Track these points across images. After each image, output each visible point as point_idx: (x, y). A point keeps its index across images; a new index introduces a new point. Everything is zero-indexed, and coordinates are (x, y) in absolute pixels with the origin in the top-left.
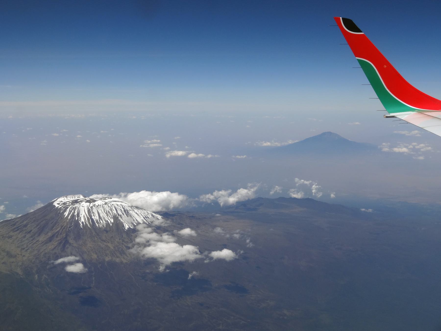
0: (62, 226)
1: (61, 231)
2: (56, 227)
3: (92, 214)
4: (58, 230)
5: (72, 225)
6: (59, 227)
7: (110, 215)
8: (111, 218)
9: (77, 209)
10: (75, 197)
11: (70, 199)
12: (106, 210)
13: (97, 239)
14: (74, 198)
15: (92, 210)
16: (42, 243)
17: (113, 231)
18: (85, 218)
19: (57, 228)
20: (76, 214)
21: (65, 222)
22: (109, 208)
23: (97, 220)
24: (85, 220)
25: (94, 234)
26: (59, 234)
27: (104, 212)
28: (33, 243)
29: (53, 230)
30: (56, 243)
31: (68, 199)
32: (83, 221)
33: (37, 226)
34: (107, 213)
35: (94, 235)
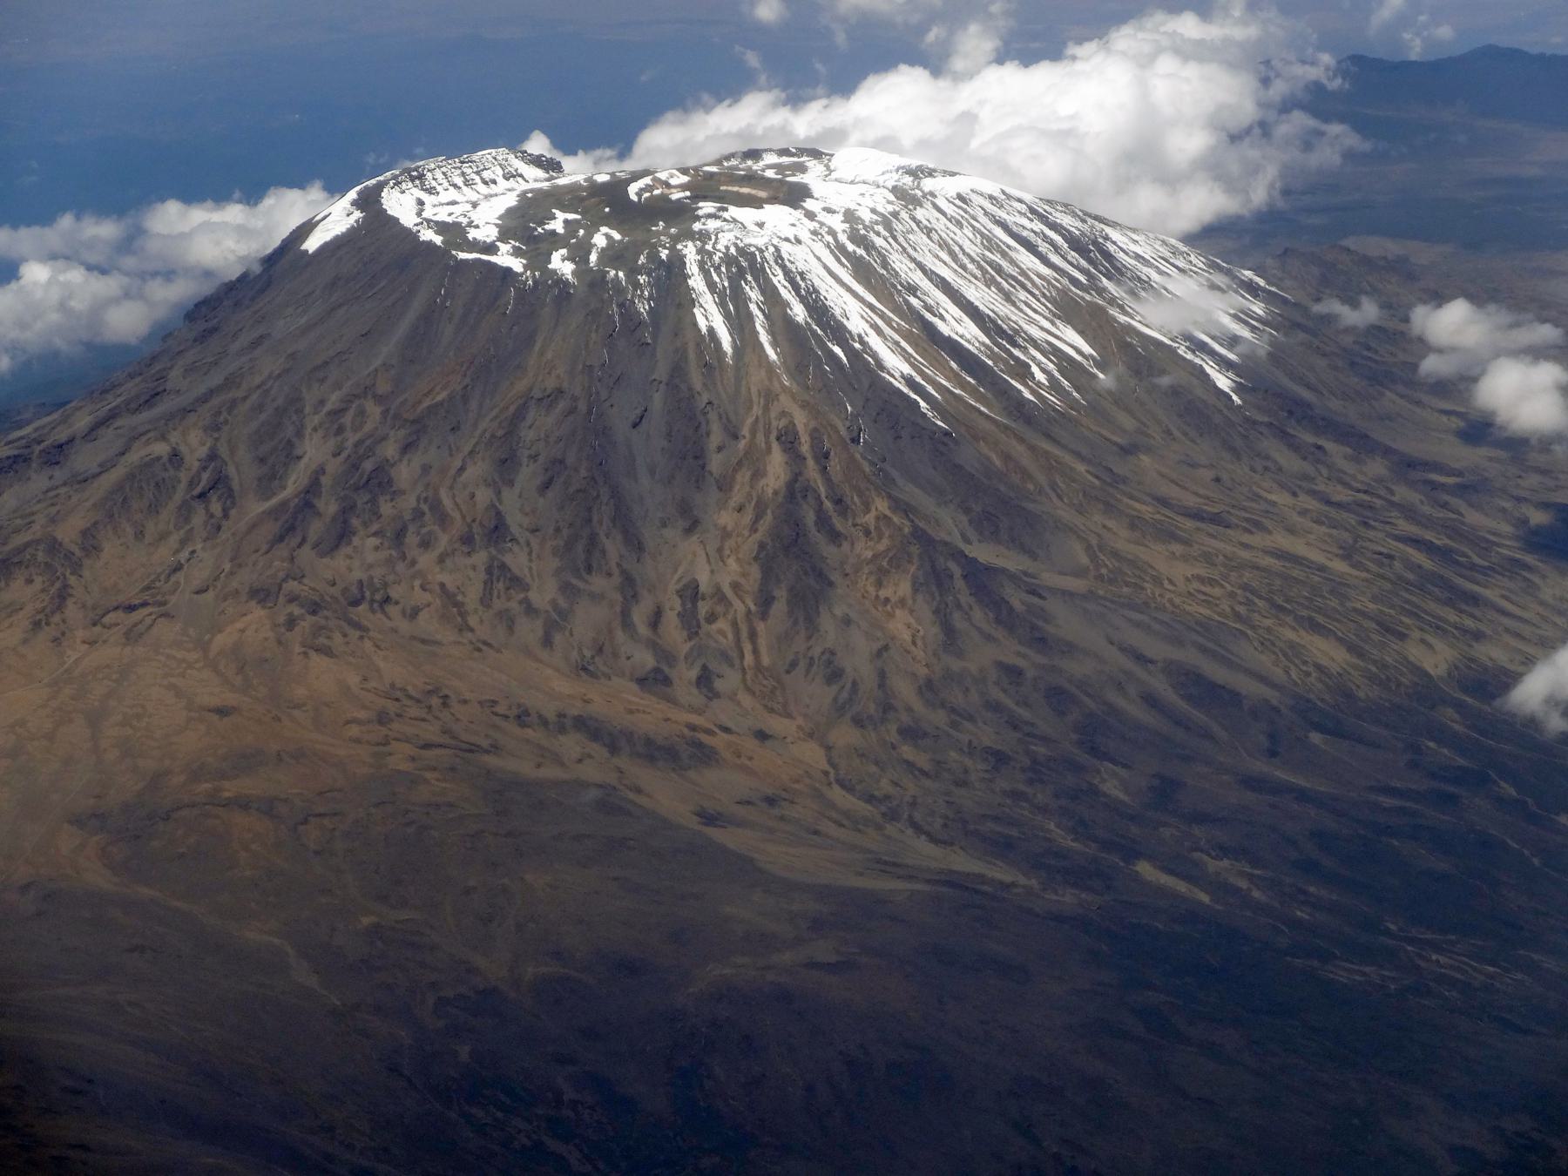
0: (788, 440)
1: (811, 469)
2: (720, 449)
3: (914, 301)
4: (777, 468)
5: (855, 416)
6: (760, 438)
7: (1023, 295)
8: (1053, 323)
9: (779, 271)
10: (486, 174)
11: (452, 194)
12: (964, 253)
13: (1149, 509)
14: (485, 182)
15: (885, 264)
16: (766, 601)
17: (1168, 432)
18: (897, 343)
19: (754, 462)
20: (799, 312)
21: (769, 397)
22: (966, 231)
23: (983, 344)
24: (907, 358)
25: (1088, 471)
26: (828, 504)
27: (964, 267)
28: (671, 619)
29: (725, 485)
30: (901, 587)
31: (445, 197)
32: (907, 369)
33: (507, 465)
34: (989, 282)
35: (1097, 482)
